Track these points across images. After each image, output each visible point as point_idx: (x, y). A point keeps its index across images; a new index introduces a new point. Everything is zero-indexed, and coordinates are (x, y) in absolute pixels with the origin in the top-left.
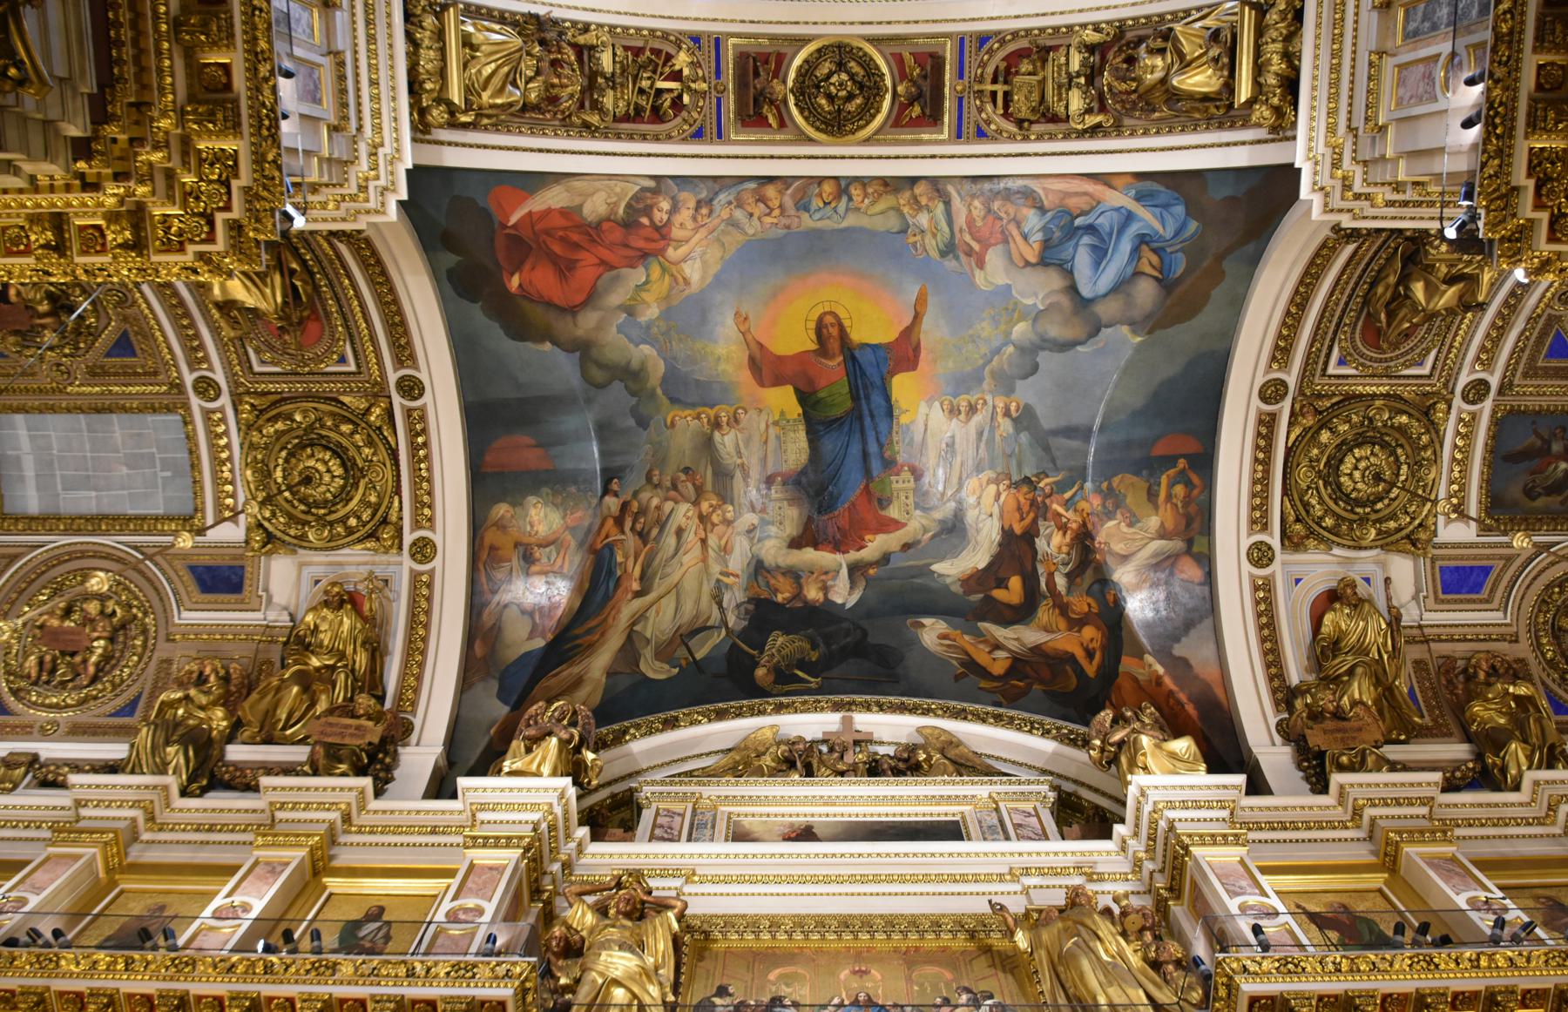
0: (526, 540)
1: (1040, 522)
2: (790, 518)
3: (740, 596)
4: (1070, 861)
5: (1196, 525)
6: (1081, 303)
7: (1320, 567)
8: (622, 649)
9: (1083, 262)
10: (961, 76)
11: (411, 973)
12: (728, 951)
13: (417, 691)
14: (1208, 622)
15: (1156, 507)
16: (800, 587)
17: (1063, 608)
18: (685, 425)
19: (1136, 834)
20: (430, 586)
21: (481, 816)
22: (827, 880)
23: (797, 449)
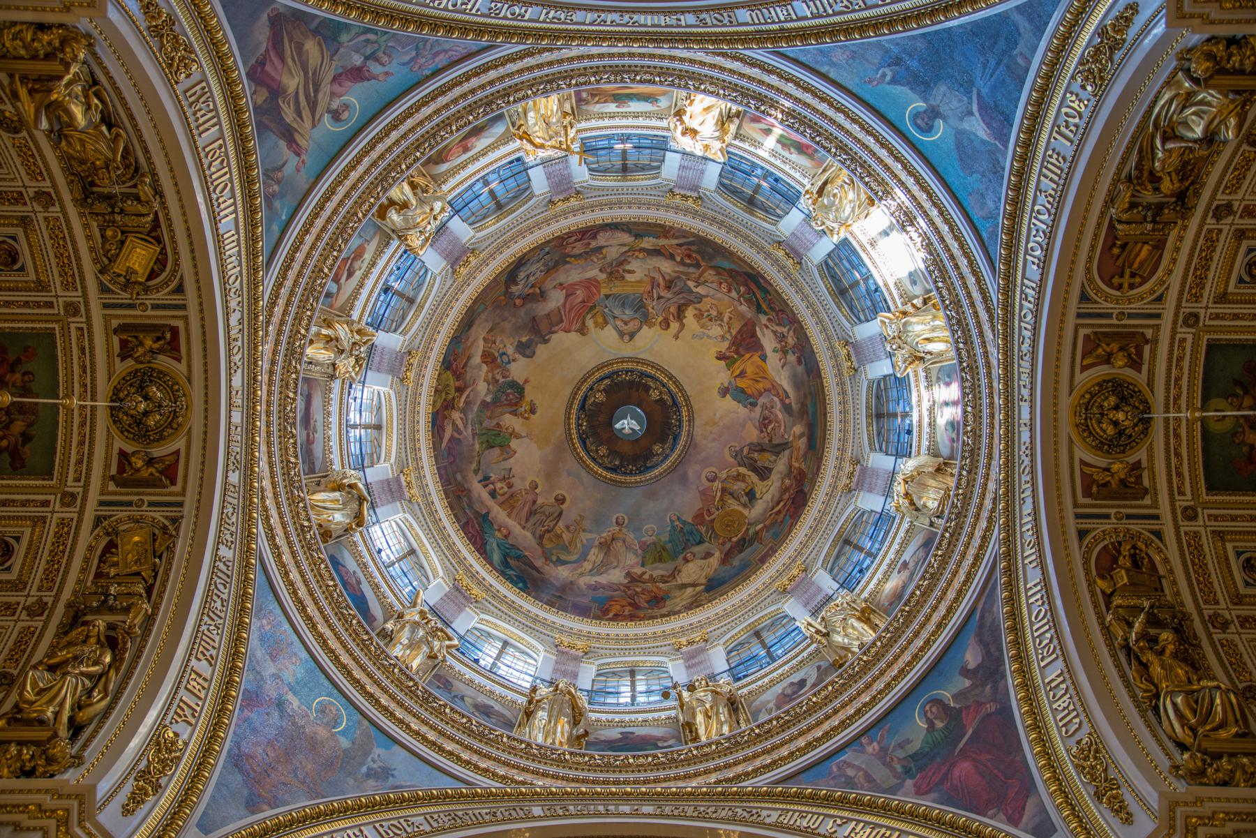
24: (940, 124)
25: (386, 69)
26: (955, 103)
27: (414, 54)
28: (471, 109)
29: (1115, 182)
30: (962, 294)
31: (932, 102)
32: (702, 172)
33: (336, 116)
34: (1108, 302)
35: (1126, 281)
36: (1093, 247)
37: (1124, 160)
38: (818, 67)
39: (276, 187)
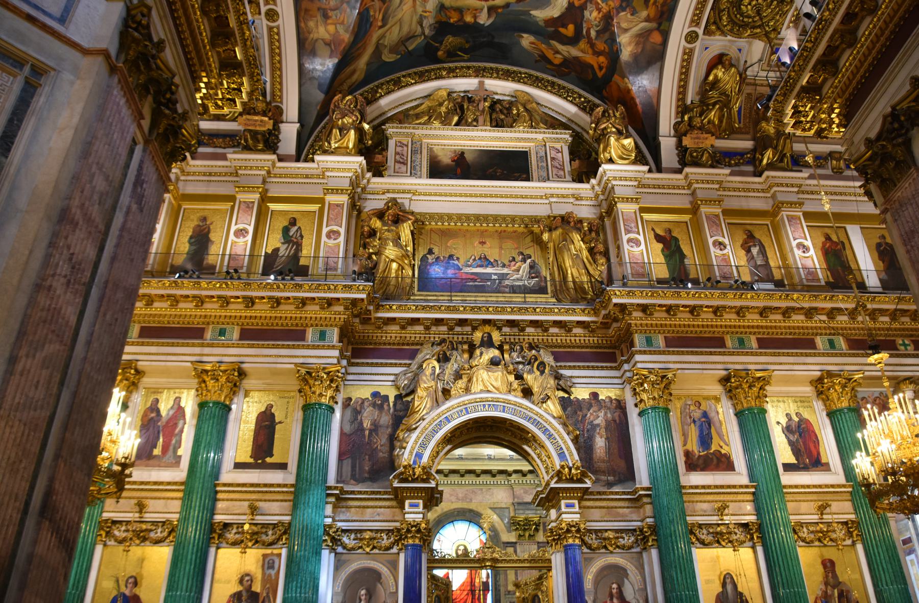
0: (324, 6)
1: (588, 4)
3: (432, 21)
4: (570, 192)
5: (665, 16)
7: (719, 43)
8: (374, 52)
11: (329, 289)
12: (431, 230)
13: (281, 90)
14: (658, 64)
15: (647, 7)
16: (462, 16)
19: (599, 184)
20: (278, 34)
21: (328, 174)
22: (471, 196)
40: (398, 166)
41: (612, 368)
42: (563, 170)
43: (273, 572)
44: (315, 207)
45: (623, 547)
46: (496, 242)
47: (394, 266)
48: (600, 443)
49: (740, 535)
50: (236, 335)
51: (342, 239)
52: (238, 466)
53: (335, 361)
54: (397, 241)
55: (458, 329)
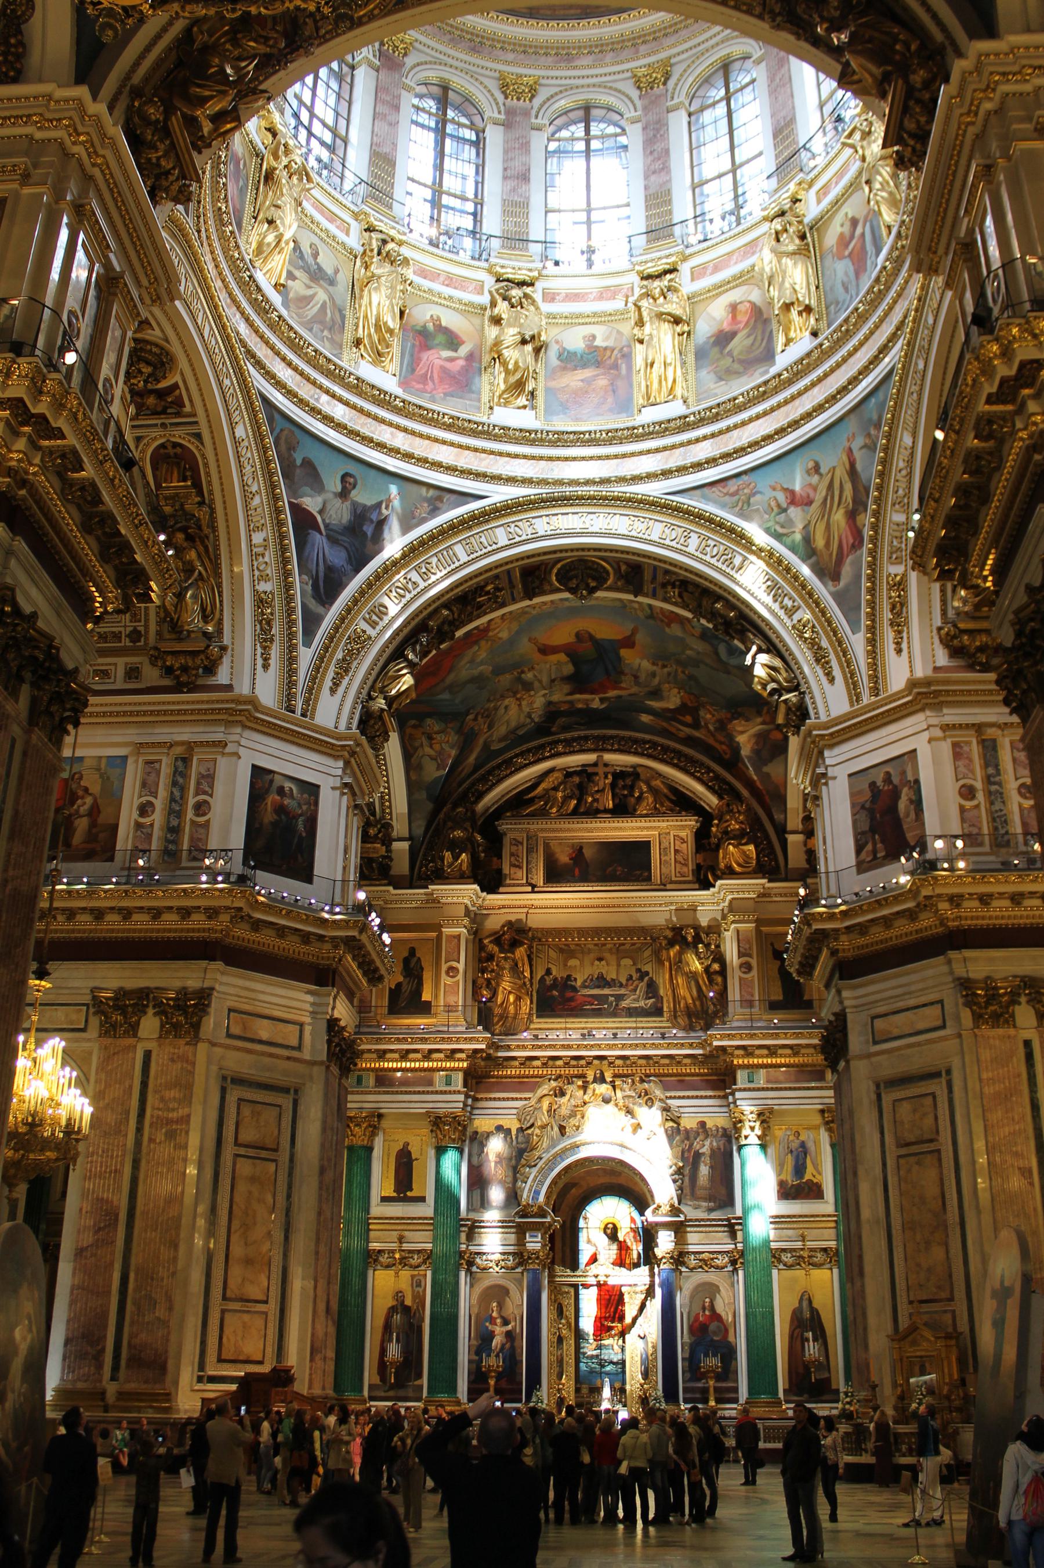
2: (567, 688)
6: (720, 660)
9: (722, 649)
10: (654, 578)
14: (782, 757)
17: (713, 735)
18: (506, 679)
23: (569, 669)
24: (339, 489)
25: (774, 494)
26: (332, 512)
27: (752, 500)
28: (716, 418)
29: (215, 530)
30: (274, 339)
31: (348, 503)
32: (505, 178)
33: (817, 468)
34: (179, 435)
35: (171, 451)
36: (208, 474)
37: (217, 548)
38: (437, 493)
39: (873, 432)
40: (513, 870)
41: (719, 1097)
42: (686, 865)
43: (421, 1290)
44: (435, 934)
45: (717, 1267)
46: (612, 959)
47: (512, 998)
48: (704, 1170)
49: (820, 1257)
50: (372, 1082)
51: (460, 977)
52: (384, 1199)
53: (461, 1105)
54: (515, 969)
55: (573, 1063)
